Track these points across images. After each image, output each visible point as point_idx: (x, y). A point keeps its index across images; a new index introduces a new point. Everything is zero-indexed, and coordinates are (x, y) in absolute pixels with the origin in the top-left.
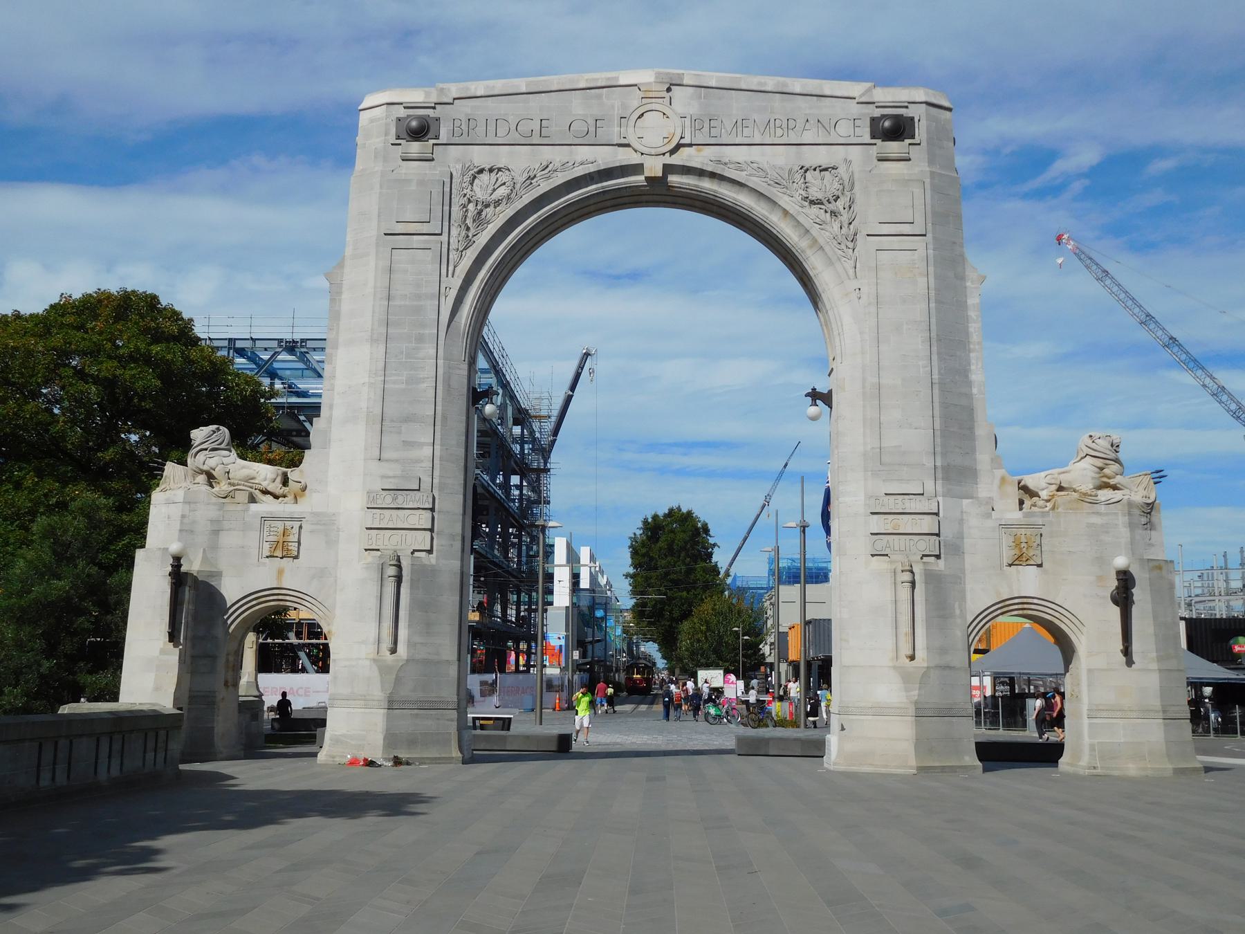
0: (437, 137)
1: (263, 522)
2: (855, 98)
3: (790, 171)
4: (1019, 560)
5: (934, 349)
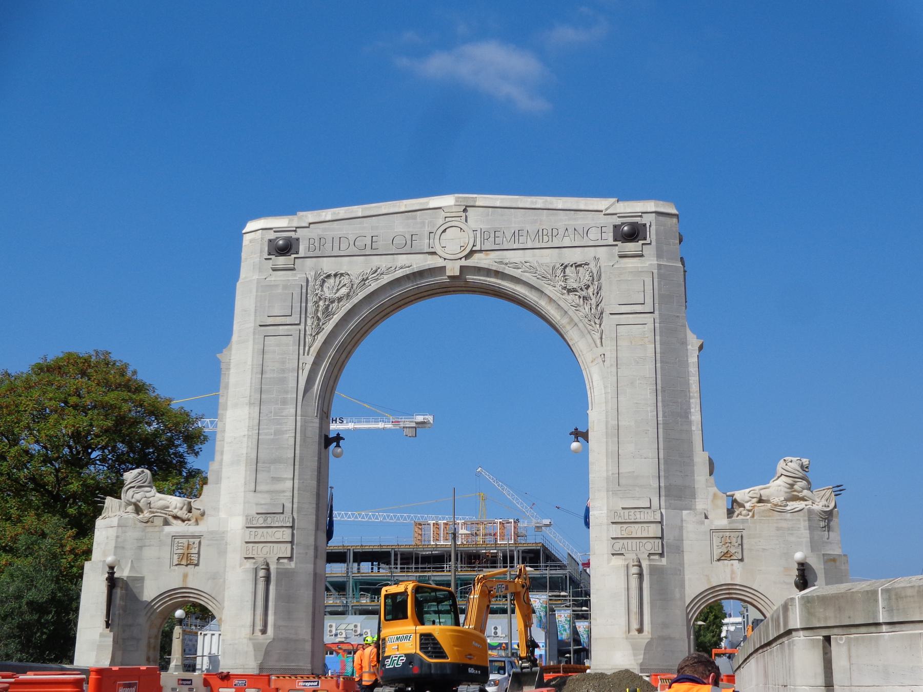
0: (297, 253)
2: (602, 211)
3: (553, 268)
4: (726, 556)
5: (660, 398)
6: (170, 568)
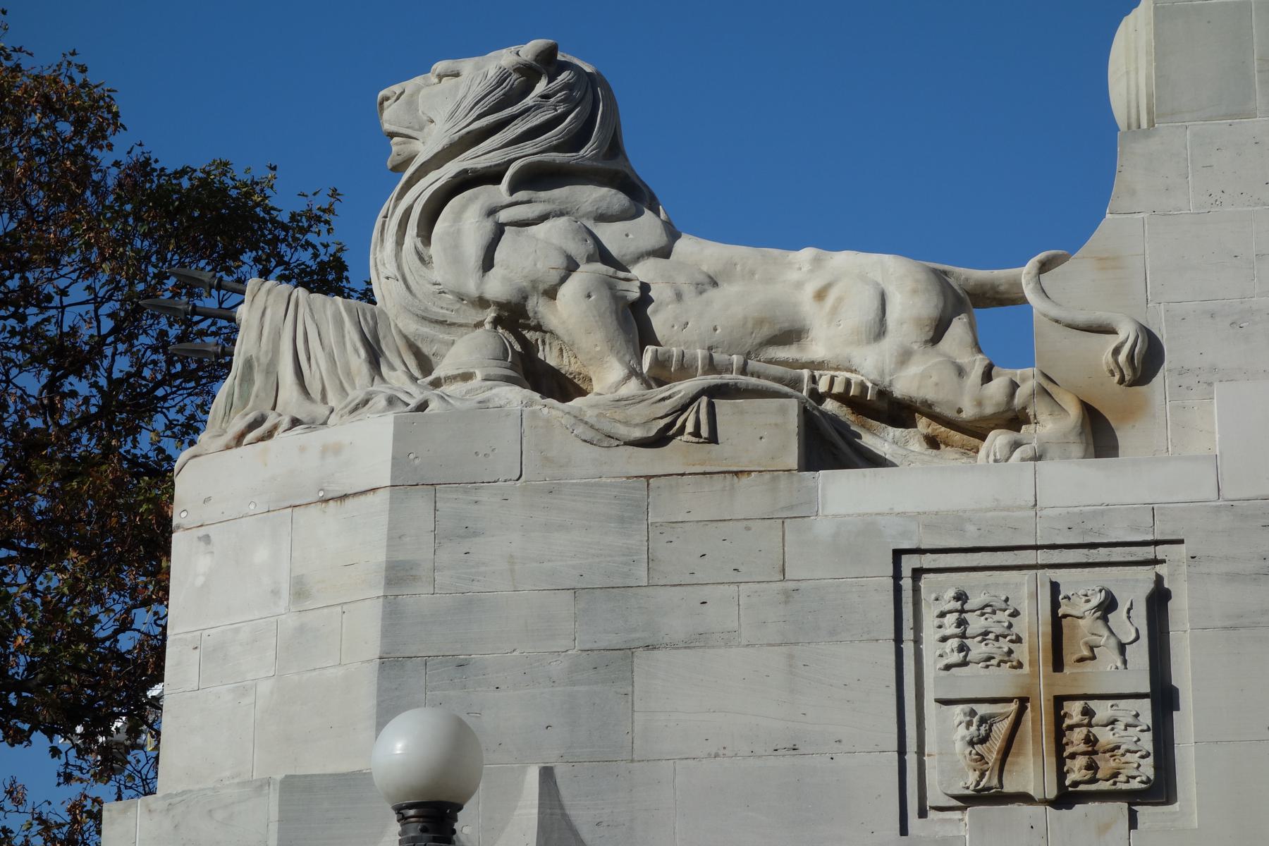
1: (907, 583)
6: (904, 831)
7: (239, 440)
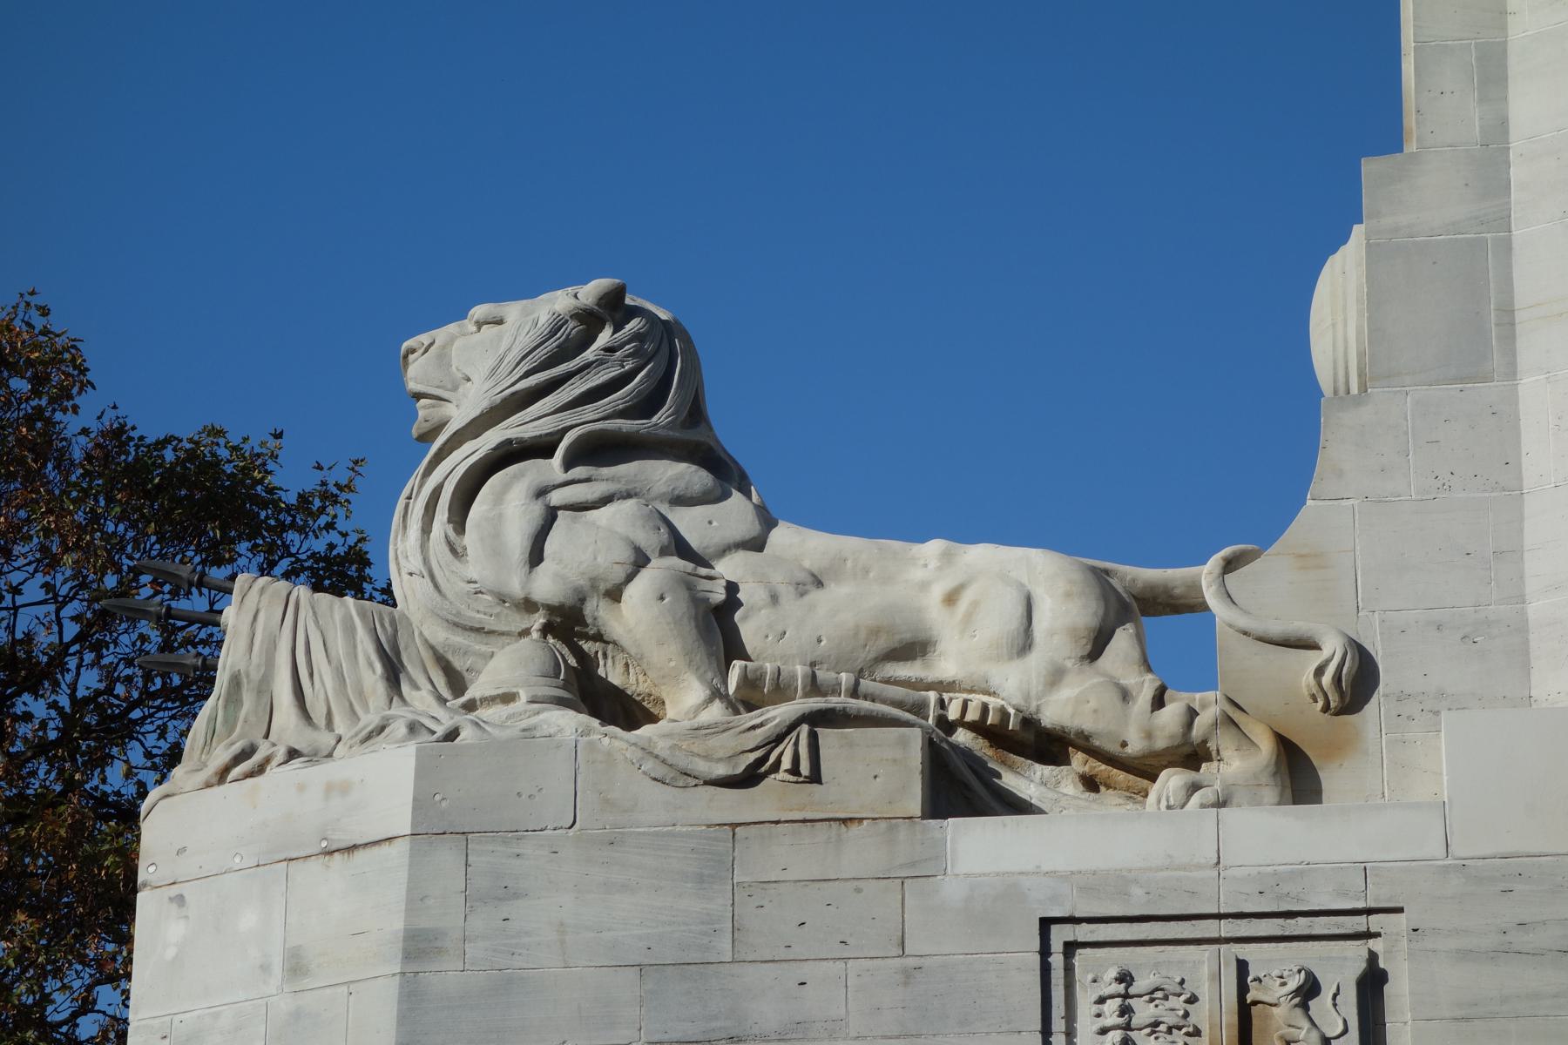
1: (1057, 960)
7: (222, 775)
